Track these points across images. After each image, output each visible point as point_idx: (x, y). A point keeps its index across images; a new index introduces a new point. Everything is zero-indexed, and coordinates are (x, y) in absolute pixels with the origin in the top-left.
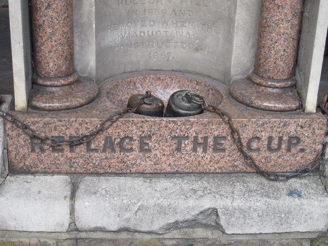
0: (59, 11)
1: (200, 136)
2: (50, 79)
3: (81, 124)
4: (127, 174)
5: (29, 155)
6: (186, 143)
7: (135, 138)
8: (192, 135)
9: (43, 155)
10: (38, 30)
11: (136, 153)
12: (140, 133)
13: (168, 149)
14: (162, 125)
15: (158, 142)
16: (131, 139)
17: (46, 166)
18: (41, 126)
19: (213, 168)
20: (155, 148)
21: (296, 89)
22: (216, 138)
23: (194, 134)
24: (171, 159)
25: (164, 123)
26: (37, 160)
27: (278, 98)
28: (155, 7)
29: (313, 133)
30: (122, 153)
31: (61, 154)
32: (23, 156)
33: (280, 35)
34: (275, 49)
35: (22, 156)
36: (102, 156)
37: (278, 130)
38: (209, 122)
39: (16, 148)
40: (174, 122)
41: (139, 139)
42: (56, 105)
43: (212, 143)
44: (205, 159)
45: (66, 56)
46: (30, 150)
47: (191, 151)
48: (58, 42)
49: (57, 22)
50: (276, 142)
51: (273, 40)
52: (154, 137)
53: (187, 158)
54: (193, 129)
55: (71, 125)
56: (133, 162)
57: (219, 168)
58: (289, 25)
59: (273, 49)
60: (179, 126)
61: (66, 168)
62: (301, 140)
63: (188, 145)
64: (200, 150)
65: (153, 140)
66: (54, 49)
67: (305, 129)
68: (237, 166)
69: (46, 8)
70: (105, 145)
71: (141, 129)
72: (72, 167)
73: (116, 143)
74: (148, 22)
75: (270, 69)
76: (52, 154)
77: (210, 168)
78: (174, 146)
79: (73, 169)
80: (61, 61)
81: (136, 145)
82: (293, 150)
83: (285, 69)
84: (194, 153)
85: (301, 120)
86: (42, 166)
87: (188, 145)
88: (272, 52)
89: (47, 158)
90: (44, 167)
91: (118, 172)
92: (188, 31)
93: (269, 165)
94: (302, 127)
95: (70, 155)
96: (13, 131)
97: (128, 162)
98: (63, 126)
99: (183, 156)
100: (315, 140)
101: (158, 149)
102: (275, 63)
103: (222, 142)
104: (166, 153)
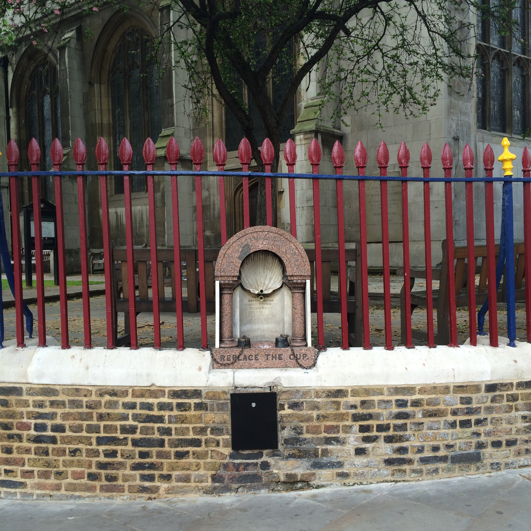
11: (254, 361)
15: (261, 356)
21: (305, 339)
27: (300, 342)
42: (228, 346)
63: (270, 357)
64: (274, 359)
82: (305, 359)
87: (270, 357)
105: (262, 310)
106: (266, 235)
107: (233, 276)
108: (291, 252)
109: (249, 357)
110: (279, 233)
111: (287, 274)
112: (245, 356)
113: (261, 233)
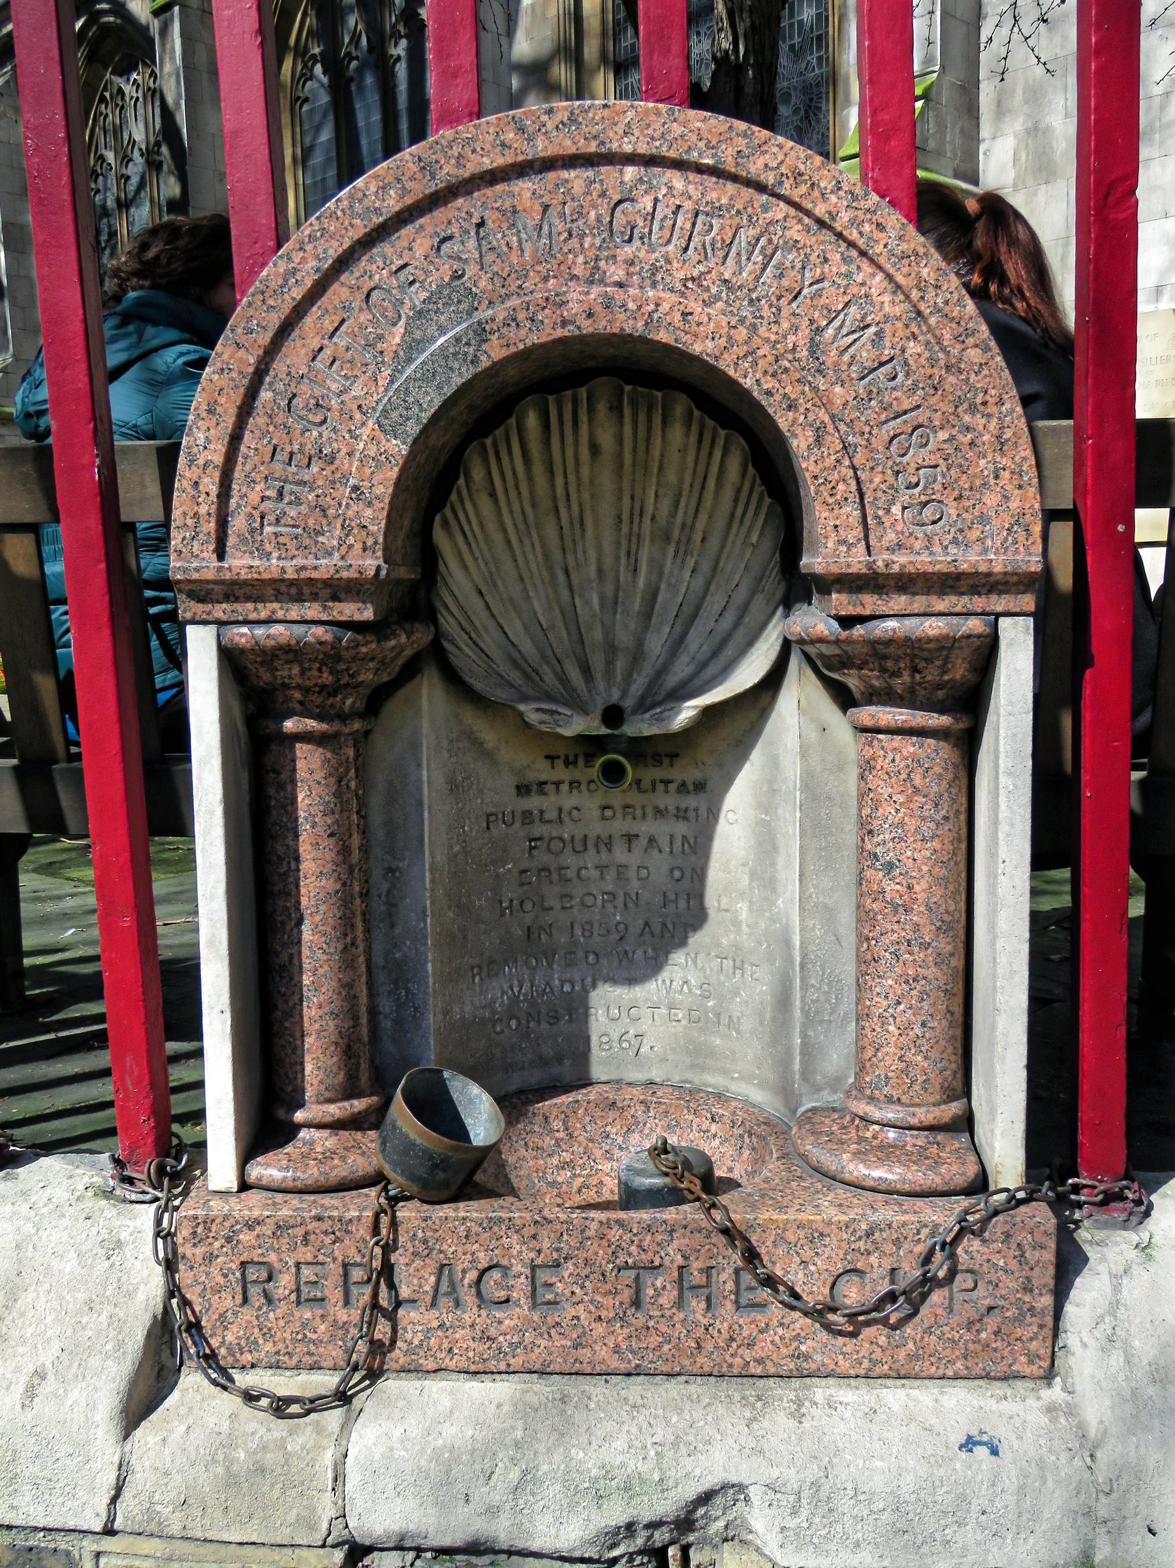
1: (696, 1265)
5: (235, 1314)
6: (659, 1283)
8: (672, 1262)
10: (277, 979)
12: (532, 1255)
13: (608, 1301)
14: (588, 1233)
16: (505, 1269)
17: (281, 1346)
18: (269, 1233)
19: (738, 1360)
20: (575, 1299)
23: (679, 1260)
25: (594, 1226)
26: (256, 1330)
29: (1021, 1258)
30: (484, 1313)
31: (320, 1312)
32: (221, 1316)
33: (906, 982)
40: (620, 1223)
41: (528, 1272)
44: (716, 1334)
46: (239, 1299)
48: (327, 1010)
53: (664, 1329)
55: (347, 1232)
57: (755, 1360)
61: (334, 1353)
63: (660, 1290)
68: (807, 1357)
73: (466, 1282)
76: (297, 1314)
77: (730, 1360)
78: (627, 1294)
81: (520, 1288)
83: (932, 1076)
84: (681, 1315)
86: (269, 1347)
88: (891, 1028)
90: (273, 1350)
93: (902, 1355)
96: (195, 1245)
97: (501, 1339)
98: (326, 1233)
99: (651, 1324)
100: (1028, 1279)
101: (582, 1301)
102: (901, 1058)
104: (604, 1314)
110: (754, 168)
113: (577, 178)
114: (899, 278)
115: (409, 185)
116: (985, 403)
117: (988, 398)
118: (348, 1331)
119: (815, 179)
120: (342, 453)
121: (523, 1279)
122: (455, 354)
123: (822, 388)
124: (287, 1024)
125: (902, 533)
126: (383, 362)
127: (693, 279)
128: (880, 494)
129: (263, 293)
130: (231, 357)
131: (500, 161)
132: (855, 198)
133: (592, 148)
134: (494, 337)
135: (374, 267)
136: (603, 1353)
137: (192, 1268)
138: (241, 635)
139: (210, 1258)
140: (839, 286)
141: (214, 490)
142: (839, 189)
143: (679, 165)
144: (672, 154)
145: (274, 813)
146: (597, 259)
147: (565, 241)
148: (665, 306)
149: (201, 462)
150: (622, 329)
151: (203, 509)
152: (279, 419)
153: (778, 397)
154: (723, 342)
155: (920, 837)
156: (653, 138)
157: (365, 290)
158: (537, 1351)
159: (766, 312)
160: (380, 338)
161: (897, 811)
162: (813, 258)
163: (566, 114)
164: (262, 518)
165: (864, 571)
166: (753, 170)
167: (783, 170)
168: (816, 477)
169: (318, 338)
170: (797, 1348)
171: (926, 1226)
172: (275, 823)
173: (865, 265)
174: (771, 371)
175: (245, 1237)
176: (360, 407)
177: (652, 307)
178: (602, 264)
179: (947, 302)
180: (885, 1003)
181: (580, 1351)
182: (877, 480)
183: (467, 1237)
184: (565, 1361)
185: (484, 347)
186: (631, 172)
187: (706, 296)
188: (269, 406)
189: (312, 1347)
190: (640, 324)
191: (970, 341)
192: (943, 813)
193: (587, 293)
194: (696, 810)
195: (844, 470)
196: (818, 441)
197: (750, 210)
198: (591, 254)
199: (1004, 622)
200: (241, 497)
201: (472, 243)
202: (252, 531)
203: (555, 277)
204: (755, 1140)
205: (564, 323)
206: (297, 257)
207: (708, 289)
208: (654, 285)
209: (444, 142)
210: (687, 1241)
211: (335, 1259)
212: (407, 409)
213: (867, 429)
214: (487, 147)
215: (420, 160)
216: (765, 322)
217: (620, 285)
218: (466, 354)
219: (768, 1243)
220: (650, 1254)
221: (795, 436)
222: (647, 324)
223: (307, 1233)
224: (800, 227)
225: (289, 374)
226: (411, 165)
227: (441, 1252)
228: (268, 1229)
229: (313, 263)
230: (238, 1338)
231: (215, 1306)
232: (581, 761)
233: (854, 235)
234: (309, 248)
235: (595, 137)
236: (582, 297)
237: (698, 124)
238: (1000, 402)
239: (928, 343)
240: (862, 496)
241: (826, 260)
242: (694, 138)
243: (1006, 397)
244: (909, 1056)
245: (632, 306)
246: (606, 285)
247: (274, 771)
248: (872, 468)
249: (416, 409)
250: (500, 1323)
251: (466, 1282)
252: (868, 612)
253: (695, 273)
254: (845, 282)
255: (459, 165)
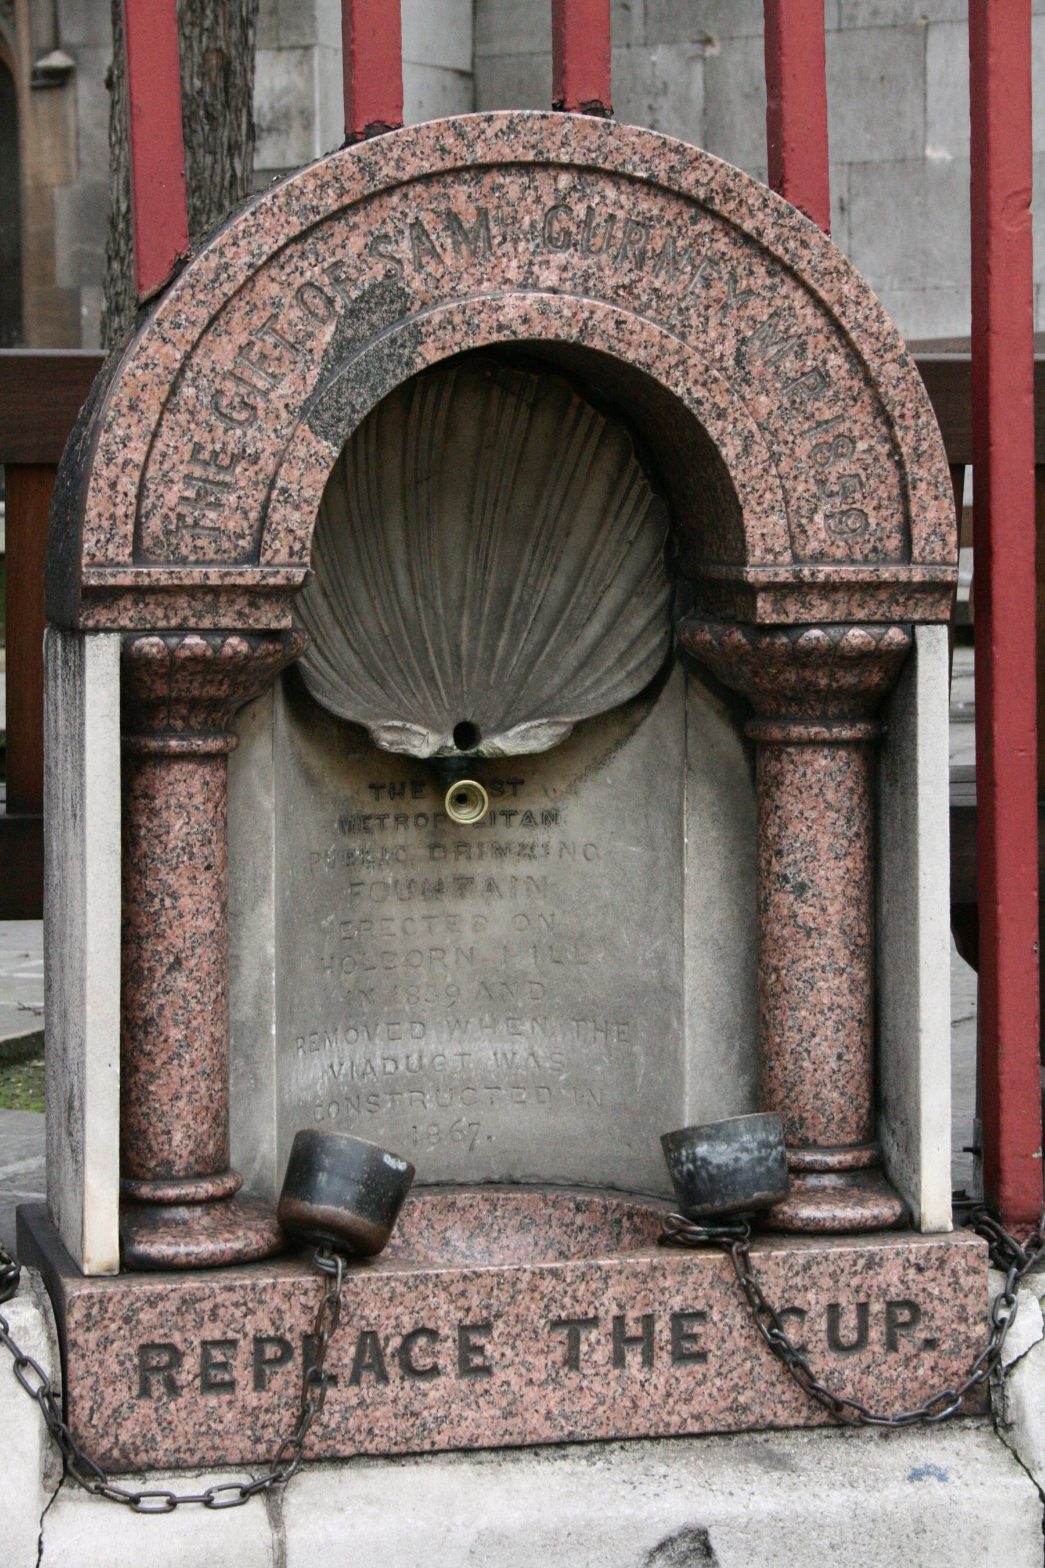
0: (203, 975)
1: (631, 1314)
2: (174, 1180)
3: (288, 1296)
4: (422, 1454)
5: (131, 1407)
6: (593, 1337)
7: (445, 1331)
8: (607, 1312)
9: (172, 1406)
11: (449, 1381)
12: (460, 1314)
13: (540, 1362)
16: (433, 1334)
17: (182, 1441)
18: (173, 1309)
19: (675, 1419)
22: (678, 1318)
24: (552, 1395)
26: (154, 1425)
27: (840, 1195)
28: (425, 980)
30: (407, 1385)
31: (226, 1397)
32: (115, 1411)
33: (822, 1012)
34: (813, 1054)
35: (110, 1412)
36: (348, 1399)
37: (855, 1282)
38: (654, 1269)
39: (94, 1389)
41: (456, 1334)
43: (666, 1335)
44: (652, 1390)
45: (217, 1111)
46: (135, 1391)
47: (610, 1366)
48: (199, 1069)
49: (199, 1008)
50: (850, 1320)
51: (804, 1028)
52: (499, 1326)
53: (597, 1387)
54: (610, 1292)
55: (261, 1302)
56: (441, 1413)
58: (842, 982)
59: (805, 1055)
60: (569, 1285)
61: (241, 1445)
62: (922, 1308)
64: (634, 1358)
65: (495, 1334)
66: (188, 1088)
67: (929, 1274)
68: (746, 1409)
69: (169, 971)
70: (358, 1360)
71: (462, 1302)
72: (258, 1440)
73: (389, 1351)
74: (406, 1026)
75: (804, 1115)
76: (201, 1402)
77: (666, 1418)
78: (559, 1354)
79: (261, 1448)
80: (206, 1126)
81: (447, 1354)
82: (906, 1346)
83: (849, 1114)
84: (617, 1372)
85: (913, 1246)
86: (169, 1444)
88: (806, 1064)
89: (183, 1414)
90: (173, 1447)
91: (395, 1449)
92: (531, 1047)
94: (920, 1269)
95: (252, 1399)
96: (88, 1329)
97: (425, 1413)
98: (236, 1305)
99: (585, 1383)
100: (963, 1308)
101: (512, 1364)
102: (817, 1096)
103: (697, 1329)
104: (535, 1376)
105: (449, 904)
106: (562, 205)
107: (257, 594)
108: (789, 365)
109: (404, 1350)
110: (686, 181)
111: (753, 574)
112: (368, 1339)
113: (512, 184)
114: (823, 294)
115: (348, 185)
116: (902, 416)
117: (905, 411)
118: (258, 1418)
119: (743, 196)
120: (267, 453)
121: (450, 1343)
122: (389, 356)
123: (748, 397)
124: (152, 1088)
125: (825, 541)
126: (313, 361)
127: (624, 287)
128: (803, 503)
129: (193, 287)
130: (157, 352)
131: (439, 166)
132: (781, 215)
133: (530, 156)
134: (430, 340)
135: (306, 264)
136: (535, 1421)
137: (83, 1356)
138: (151, 645)
139: (105, 1343)
140: (764, 298)
141: (133, 491)
142: (766, 206)
143: (615, 176)
144: (608, 166)
145: (144, 844)
146: (531, 263)
147: (500, 244)
148: (599, 315)
149: (120, 460)
150: (557, 335)
151: (120, 511)
152: (203, 416)
153: (707, 406)
154: (655, 351)
155: (833, 855)
156: (589, 150)
157: (296, 286)
158: (464, 1424)
159: (695, 321)
160: (310, 335)
161: (809, 828)
162: (740, 270)
163: (506, 123)
164: (178, 519)
165: (791, 580)
166: (684, 185)
167: (714, 186)
168: (744, 486)
169: (246, 334)
170: (735, 1400)
171: (862, 1256)
172: (145, 856)
173: (790, 283)
174: (701, 380)
175: (147, 1316)
176: (287, 406)
177: (586, 314)
178: (536, 269)
179: (866, 318)
180: (798, 1037)
181: (510, 1421)
182: (801, 488)
183: (391, 1299)
184: (494, 1434)
185: (420, 349)
186: (565, 180)
187: (636, 304)
188: (191, 403)
189: (217, 1441)
190: (575, 332)
191: (889, 356)
192: (855, 829)
193: (524, 298)
194: (546, 846)
195: (770, 479)
196: (746, 450)
197: (679, 222)
198: (525, 259)
199: (921, 631)
200: (158, 498)
201: (405, 244)
202: (168, 533)
203: (489, 280)
204: (637, 1220)
205: (500, 328)
206: (230, 252)
207: (638, 297)
208: (586, 292)
209: (385, 145)
210: (621, 1288)
211: (246, 1335)
212: (340, 409)
213: (791, 438)
214: (427, 151)
215: (360, 160)
216: (693, 331)
217: (554, 291)
218: (401, 356)
219: (705, 1285)
220: (585, 1305)
221: (725, 445)
222: (581, 331)
223: (216, 1307)
224: (727, 240)
225: (213, 370)
226: (350, 165)
227: (362, 1317)
228: (171, 1306)
229: (247, 259)
230: (134, 1436)
231: (108, 1399)
232: (408, 793)
233: (780, 251)
234: (243, 243)
235: (533, 147)
236: (518, 303)
237: (633, 139)
238: (917, 416)
239: (847, 356)
240: (787, 503)
241: (752, 273)
242: (628, 151)
243: (921, 410)
244: (825, 1092)
245: (567, 313)
246: (540, 290)
247: (146, 796)
248: (796, 477)
249: (348, 410)
250: (425, 1395)
251: (389, 1351)
252: (791, 620)
253: (627, 281)
254: (769, 295)
255: (398, 167)
